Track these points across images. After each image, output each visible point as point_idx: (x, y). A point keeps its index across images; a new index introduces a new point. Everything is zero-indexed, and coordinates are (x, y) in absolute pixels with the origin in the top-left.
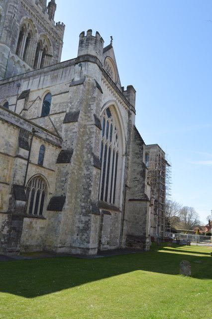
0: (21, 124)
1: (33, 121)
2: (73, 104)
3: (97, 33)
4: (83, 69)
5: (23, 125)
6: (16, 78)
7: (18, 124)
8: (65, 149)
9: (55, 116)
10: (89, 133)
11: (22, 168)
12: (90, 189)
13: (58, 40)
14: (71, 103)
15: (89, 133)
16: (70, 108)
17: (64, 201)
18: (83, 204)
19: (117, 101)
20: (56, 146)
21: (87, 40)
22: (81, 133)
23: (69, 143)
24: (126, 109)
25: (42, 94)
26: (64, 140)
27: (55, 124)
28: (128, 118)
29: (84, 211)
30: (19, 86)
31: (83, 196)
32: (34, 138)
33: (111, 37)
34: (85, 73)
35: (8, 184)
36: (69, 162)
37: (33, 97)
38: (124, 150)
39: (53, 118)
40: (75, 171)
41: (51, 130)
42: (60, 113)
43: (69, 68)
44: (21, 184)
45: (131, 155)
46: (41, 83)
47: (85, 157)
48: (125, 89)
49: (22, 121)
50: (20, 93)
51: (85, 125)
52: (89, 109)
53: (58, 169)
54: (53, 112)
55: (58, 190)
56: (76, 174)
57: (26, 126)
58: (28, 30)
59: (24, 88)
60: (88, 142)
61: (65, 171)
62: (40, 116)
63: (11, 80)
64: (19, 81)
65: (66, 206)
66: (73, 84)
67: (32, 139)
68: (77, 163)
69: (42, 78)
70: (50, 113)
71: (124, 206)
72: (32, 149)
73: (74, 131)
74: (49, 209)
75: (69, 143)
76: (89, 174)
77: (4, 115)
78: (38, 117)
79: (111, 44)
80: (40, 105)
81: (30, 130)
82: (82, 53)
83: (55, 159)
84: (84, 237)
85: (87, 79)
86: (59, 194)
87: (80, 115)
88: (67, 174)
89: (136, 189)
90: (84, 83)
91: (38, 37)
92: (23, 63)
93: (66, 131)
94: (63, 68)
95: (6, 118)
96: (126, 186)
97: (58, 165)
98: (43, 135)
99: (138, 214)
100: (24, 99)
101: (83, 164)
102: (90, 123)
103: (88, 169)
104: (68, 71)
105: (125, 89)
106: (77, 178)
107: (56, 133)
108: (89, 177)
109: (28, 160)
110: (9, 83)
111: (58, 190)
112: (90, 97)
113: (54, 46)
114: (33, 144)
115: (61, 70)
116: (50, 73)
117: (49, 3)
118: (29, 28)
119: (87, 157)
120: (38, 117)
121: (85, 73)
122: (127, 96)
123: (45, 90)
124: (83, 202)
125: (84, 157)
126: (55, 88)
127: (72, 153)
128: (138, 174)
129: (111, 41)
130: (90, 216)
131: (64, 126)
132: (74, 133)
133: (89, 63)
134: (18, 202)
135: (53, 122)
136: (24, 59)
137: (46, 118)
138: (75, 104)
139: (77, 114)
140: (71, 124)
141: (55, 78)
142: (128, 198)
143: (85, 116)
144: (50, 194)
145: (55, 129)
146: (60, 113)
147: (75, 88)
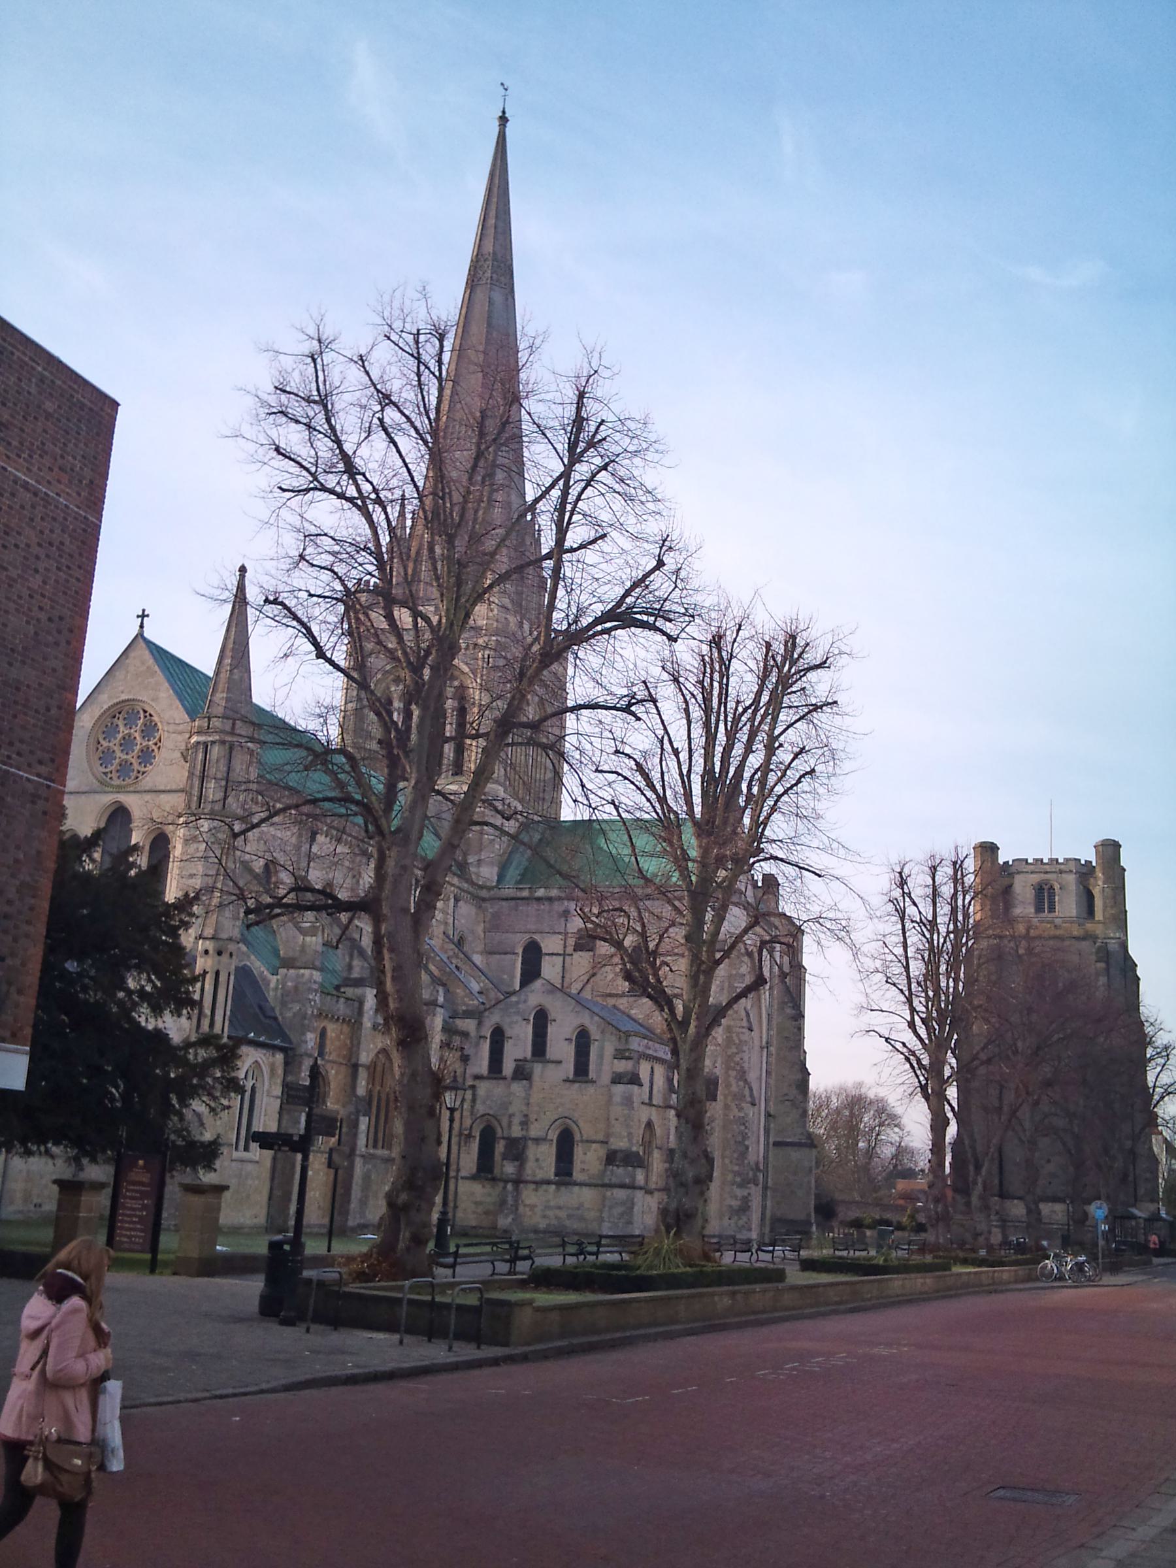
10: (737, 1041)
12: (746, 1143)
15: (737, 1041)
18: (736, 1168)
29: (738, 1179)
31: (735, 1155)
38: (764, 1036)
71: (766, 1158)
84: (741, 1223)
89: (789, 1120)
96: (768, 1115)
102: (739, 1023)
103: (741, 1109)
108: (743, 1121)
119: (738, 1086)
124: (737, 1164)
125: (731, 1086)
130: (750, 1188)
142: (771, 1140)
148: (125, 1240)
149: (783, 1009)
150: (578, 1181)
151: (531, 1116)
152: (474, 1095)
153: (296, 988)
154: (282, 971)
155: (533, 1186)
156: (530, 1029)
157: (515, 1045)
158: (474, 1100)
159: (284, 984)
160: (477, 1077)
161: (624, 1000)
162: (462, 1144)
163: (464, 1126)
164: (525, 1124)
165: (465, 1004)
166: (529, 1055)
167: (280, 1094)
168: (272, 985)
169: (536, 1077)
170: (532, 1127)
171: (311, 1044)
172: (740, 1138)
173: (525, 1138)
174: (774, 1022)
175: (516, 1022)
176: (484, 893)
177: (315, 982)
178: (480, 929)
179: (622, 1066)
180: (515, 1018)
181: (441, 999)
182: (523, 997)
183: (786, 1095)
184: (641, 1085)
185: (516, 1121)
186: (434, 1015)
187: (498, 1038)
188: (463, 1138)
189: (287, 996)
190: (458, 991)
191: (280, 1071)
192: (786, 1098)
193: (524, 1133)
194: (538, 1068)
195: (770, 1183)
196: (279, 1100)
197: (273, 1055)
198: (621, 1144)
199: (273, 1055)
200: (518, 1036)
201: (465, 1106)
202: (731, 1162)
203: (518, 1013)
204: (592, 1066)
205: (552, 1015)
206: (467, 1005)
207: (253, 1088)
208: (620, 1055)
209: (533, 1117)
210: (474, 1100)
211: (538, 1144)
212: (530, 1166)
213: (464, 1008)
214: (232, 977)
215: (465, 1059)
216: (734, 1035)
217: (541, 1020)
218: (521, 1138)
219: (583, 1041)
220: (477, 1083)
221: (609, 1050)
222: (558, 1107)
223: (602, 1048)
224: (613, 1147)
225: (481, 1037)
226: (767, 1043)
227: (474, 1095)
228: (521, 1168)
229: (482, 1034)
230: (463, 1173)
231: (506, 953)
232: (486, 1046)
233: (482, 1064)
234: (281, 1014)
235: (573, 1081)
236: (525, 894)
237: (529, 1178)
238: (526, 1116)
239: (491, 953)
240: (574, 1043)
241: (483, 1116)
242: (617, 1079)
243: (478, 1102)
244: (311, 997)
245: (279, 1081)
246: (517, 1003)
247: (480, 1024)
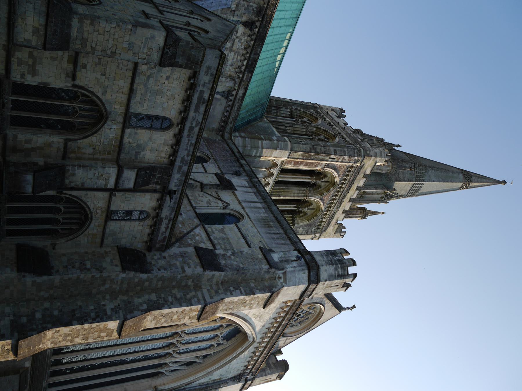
0: (180, 167)
1: (185, 201)
2: (233, 257)
3: (355, 276)
4: (295, 264)
5: (179, 171)
6: (247, 168)
7: (178, 163)
8: (149, 259)
9: (204, 235)
10: (188, 296)
11: (98, 178)
13: (319, 230)
14: (233, 254)
15: (188, 296)
16: (224, 255)
17: (40, 275)
18: (38, 315)
19: (256, 345)
20: (151, 240)
21: (338, 260)
22: (183, 284)
23: (162, 262)
24: (246, 366)
25: (235, 206)
26: (165, 254)
27: (189, 236)
28: (230, 376)
29: (24, 320)
30: (237, 174)
31: (56, 313)
32: (157, 196)
33: (354, 307)
34: (289, 268)
35: (64, 157)
36: (124, 269)
37: (226, 196)
39: (199, 230)
40: (107, 286)
41: (177, 231)
42: (211, 240)
43: (288, 242)
44: (67, 181)
46: (252, 205)
47: (140, 300)
48: (279, 358)
49: (185, 168)
50: (227, 176)
51: (200, 288)
52: (232, 289)
53: (106, 252)
54: (209, 230)
56: (102, 288)
57: (176, 177)
58: (319, 182)
59: (235, 181)
60: (170, 299)
61: (104, 265)
62: (198, 211)
63: (243, 162)
64: (244, 174)
65: (29, 279)
66: (266, 253)
67: (155, 191)
68: (125, 286)
69: (259, 205)
70: (206, 226)
72: (138, 194)
73: (186, 268)
74: (20, 248)
75: (162, 262)
76: (106, 314)
77: (188, 136)
78: (194, 208)
79: (344, 309)
80: (216, 208)
81: (172, 186)
82: (318, 258)
83: (124, 242)
85: (280, 273)
87: (217, 273)
88: (101, 270)
90: (273, 270)
91: (315, 199)
92: (271, 181)
93: (183, 255)
94: (286, 233)
95: (185, 140)
98: (165, 212)
100: (218, 183)
101: (125, 298)
104: (283, 242)
105: (279, 358)
106: (94, 291)
107: (173, 240)
109: (116, 189)
110: (238, 160)
112: (252, 285)
113: (310, 225)
114: (148, 196)
115: (281, 231)
116: (272, 216)
117: (364, 209)
118: (323, 184)
119: (141, 304)
120: (194, 208)
121: (289, 268)
122: (268, 365)
123: (242, 212)
125: (139, 297)
126: (249, 226)
127: (142, 272)
129: (348, 308)
131: (191, 250)
132: (183, 268)
133: (306, 271)
134: (29, 177)
135: (192, 233)
136: (277, 183)
137: (196, 221)
138: (235, 262)
139: (218, 268)
140: (197, 261)
141: (265, 223)
143: (217, 284)
144: (54, 246)
145: (182, 238)
146: (211, 240)
147: (260, 256)
161: (189, 208)
172: (78, 314)
176: (227, 136)
216: (193, 293)
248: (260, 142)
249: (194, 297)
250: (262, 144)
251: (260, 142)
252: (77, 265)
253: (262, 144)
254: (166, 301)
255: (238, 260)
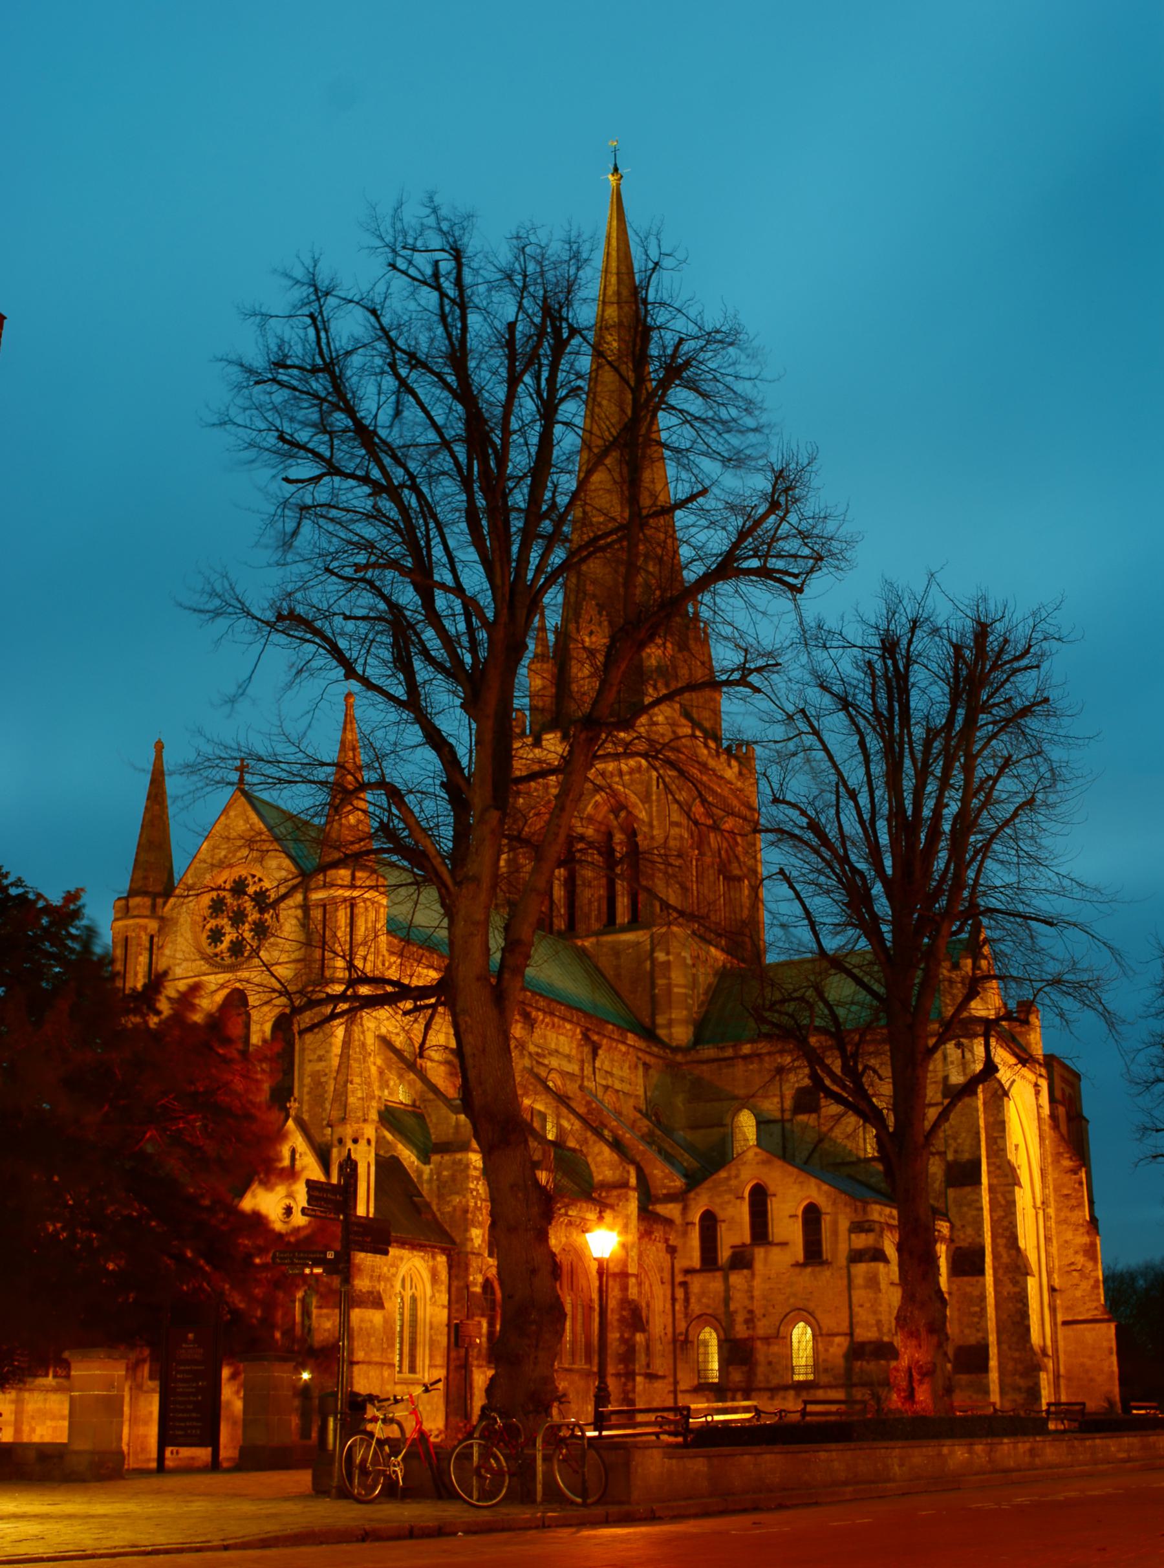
2: (959, 1141)
10: (1003, 1202)
15: (1003, 1202)
16: (956, 1152)
18: (1017, 1355)
45: (1052, 1203)
52: (995, 1147)
53: (959, 1289)
55: (967, 1331)
60: (1005, 1223)
71: (1055, 1341)
86: (972, 1340)
89: (1079, 1294)
96: (1052, 1290)
97: (958, 1280)
99: (1091, 1357)
111: (967, 1331)
119: (1009, 1256)
128: (1076, 1252)
142: (1060, 1318)
148: (180, 1433)
149: (1058, 1162)
150: (822, 1384)
151: (757, 1312)
152: (687, 1294)
153: (453, 1178)
154: (436, 1158)
155: (768, 1394)
156: (745, 1208)
157: (729, 1229)
158: (687, 1300)
159: (439, 1174)
160: (688, 1271)
162: (678, 1352)
163: (678, 1331)
164: (750, 1321)
165: (664, 1187)
166: (747, 1239)
167: (446, 1303)
168: (426, 1176)
169: (758, 1265)
170: (759, 1324)
171: (477, 1242)
173: (751, 1339)
174: (1050, 1178)
175: (729, 1202)
177: (475, 1168)
178: (679, 1101)
179: (861, 1241)
180: (727, 1197)
181: (633, 1181)
182: (734, 1172)
183: (1072, 1264)
184: (886, 1260)
185: (740, 1318)
186: (627, 1200)
187: (709, 1223)
188: (678, 1344)
189: (444, 1187)
190: (656, 1172)
191: (444, 1275)
192: (1073, 1267)
193: (751, 1332)
194: (759, 1253)
195: (1062, 1371)
196: (446, 1311)
197: (434, 1258)
198: (870, 1335)
199: (434, 1258)
200: (733, 1218)
201: (677, 1307)
202: (1010, 1348)
203: (730, 1191)
204: (826, 1246)
205: (772, 1189)
206: (669, 1188)
207: (414, 1299)
208: (858, 1227)
209: (758, 1312)
210: (687, 1300)
211: (769, 1344)
212: (761, 1370)
213: (665, 1191)
214: (373, 1168)
215: (672, 1250)
217: (760, 1198)
218: (747, 1339)
219: (812, 1216)
220: (688, 1278)
221: (844, 1224)
222: (788, 1298)
223: (835, 1223)
224: (860, 1339)
225: (688, 1224)
226: (1043, 1203)
227: (687, 1294)
228: (751, 1374)
229: (690, 1219)
230: (682, 1386)
231: (712, 1126)
232: (695, 1237)
233: (693, 1255)
234: (439, 1210)
235: (804, 1265)
236: (729, 1053)
237: (762, 1385)
238: (751, 1312)
239: (694, 1127)
240: (800, 1219)
241: (699, 1317)
242: (857, 1256)
243: (693, 1300)
244: (472, 1186)
245: (444, 1288)
246: (728, 1179)
247: (685, 1210)
248: (676, 990)
249: (1004, 1196)
250: (678, 986)
251: (676, 990)
252: (976, 1320)
253: (678, 986)
254: (1006, 1229)
255: (964, 1135)
